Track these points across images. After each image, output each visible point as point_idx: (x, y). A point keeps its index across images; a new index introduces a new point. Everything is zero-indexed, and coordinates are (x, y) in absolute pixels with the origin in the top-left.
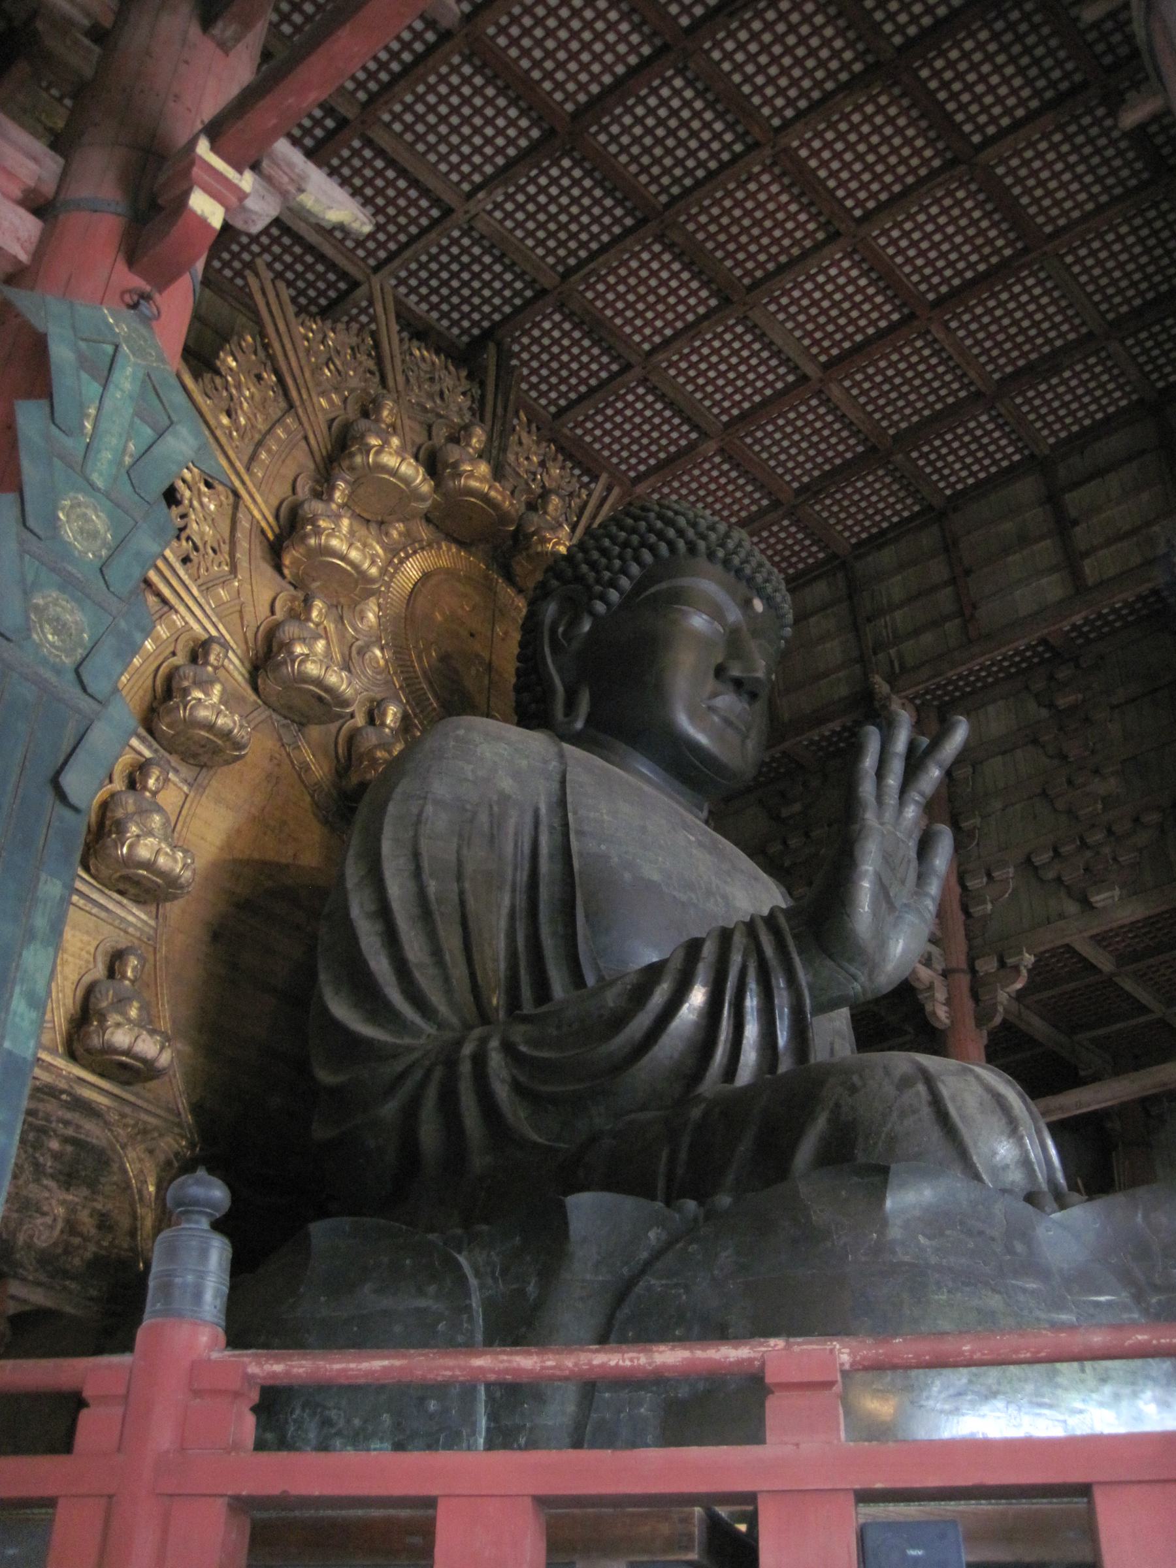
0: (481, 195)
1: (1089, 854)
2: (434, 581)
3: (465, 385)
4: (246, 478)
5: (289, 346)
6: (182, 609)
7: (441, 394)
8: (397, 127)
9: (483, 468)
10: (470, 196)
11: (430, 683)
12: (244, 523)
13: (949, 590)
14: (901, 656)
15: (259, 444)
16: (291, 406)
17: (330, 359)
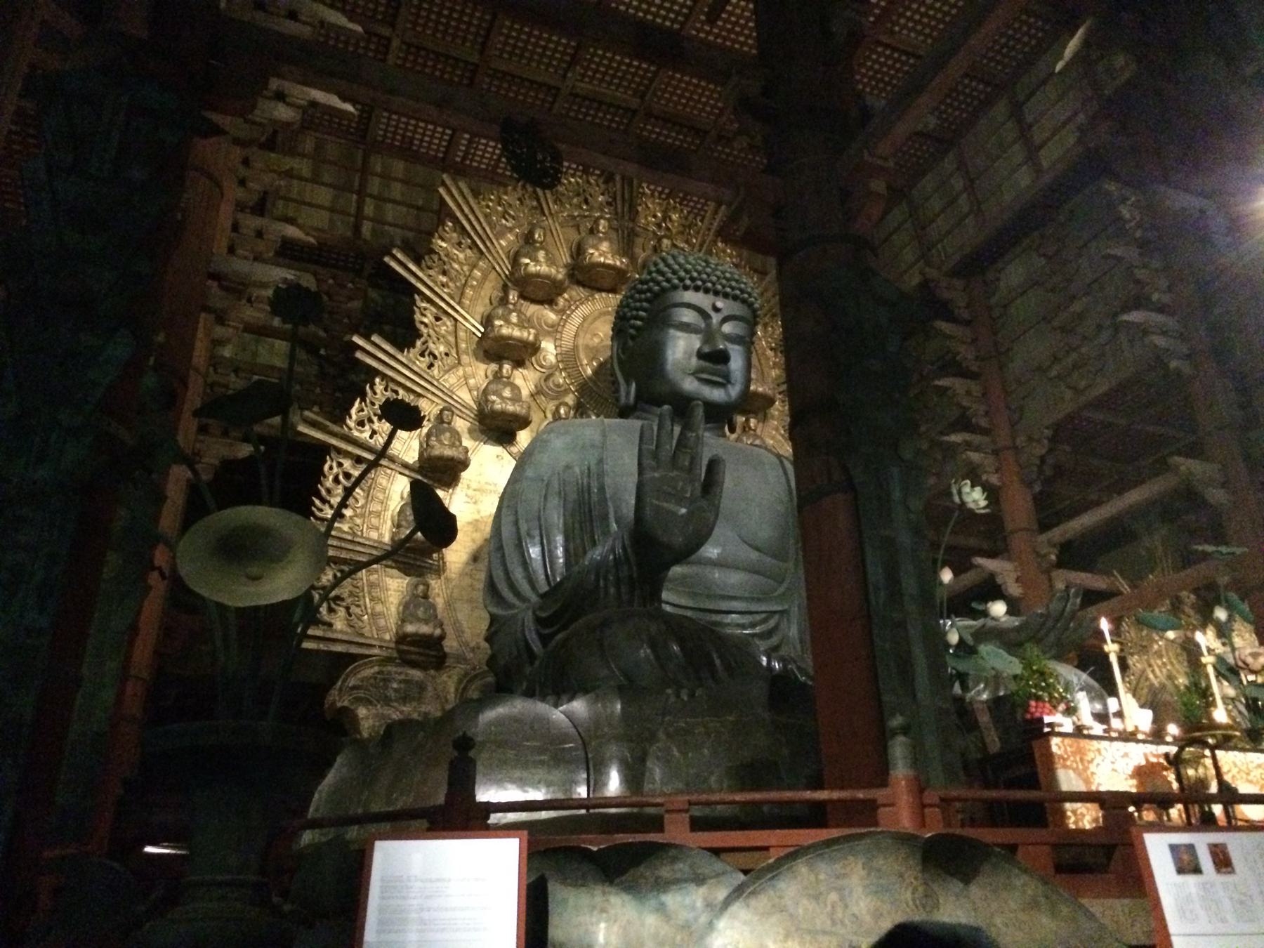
0: (569, 75)
1: (1074, 355)
2: (590, 320)
3: (603, 186)
4: (458, 308)
5: (471, 217)
6: (429, 396)
7: (586, 202)
8: (506, 56)
9: (605, 246)
10: (564, 76)
11: (595, 383)
12: (462, 334)
13: (965, 195)
14: (944, 247)
15: (465, 285)
16: (481, 252)
17: (506, 212)
